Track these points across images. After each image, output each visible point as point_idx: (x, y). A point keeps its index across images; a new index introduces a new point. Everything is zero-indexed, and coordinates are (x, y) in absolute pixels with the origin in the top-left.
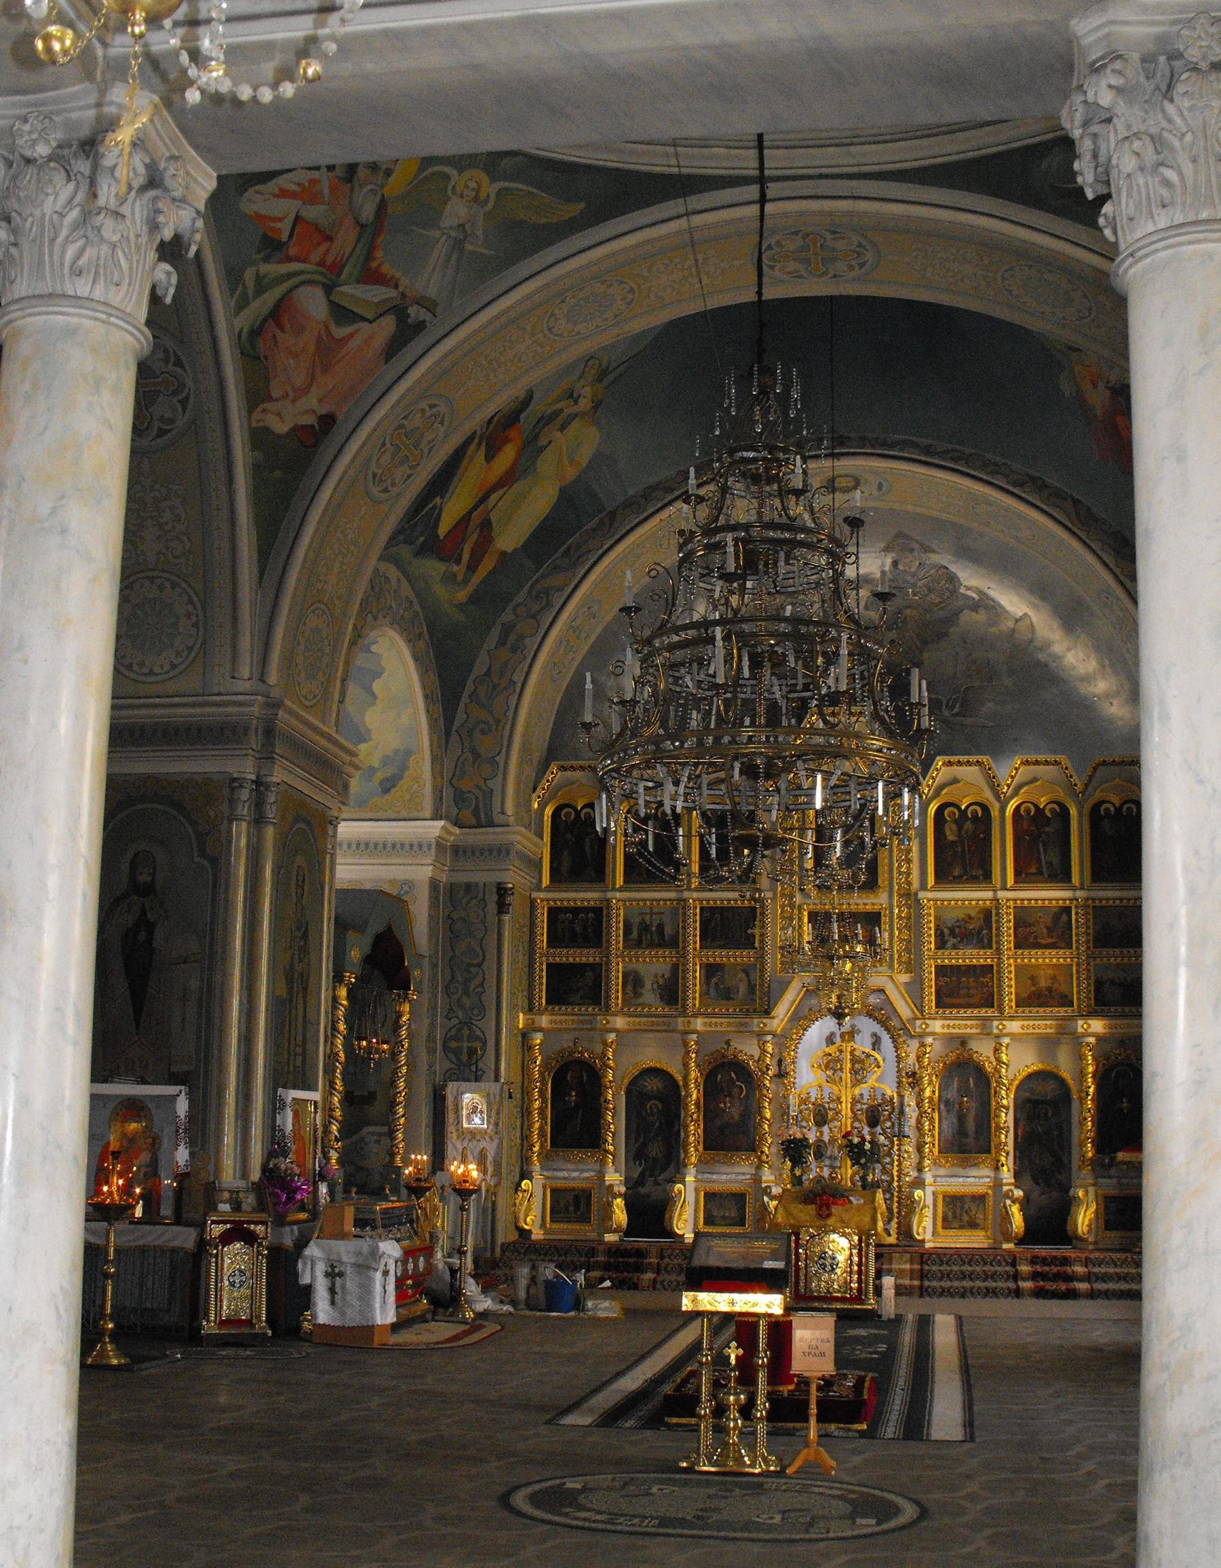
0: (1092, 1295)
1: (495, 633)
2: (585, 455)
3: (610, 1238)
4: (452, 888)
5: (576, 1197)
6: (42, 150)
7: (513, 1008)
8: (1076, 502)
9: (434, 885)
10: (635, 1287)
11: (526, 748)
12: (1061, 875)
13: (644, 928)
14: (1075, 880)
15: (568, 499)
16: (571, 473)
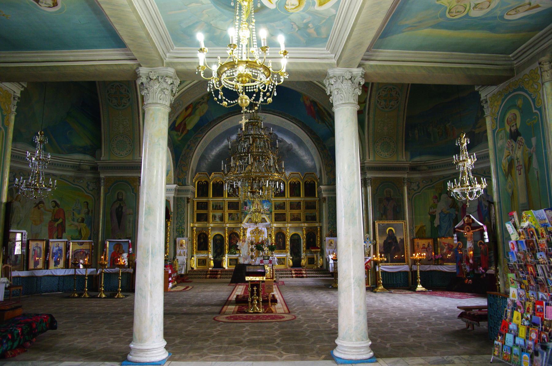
0: (307, 277)
1: (186, 146)
2: (205, 111)
3: (210, 269)
4: (178, 198)
5: (203, 261)
6: (155, 78)
7: (190, 222)
8: (303, 123)
9: (174, 197)
10: (216, 278)
11: (192, 170)
12: (299, 195)
13: (216, 206)
14: (302, 196)
15: (201, 119)
16: (202, 114)
